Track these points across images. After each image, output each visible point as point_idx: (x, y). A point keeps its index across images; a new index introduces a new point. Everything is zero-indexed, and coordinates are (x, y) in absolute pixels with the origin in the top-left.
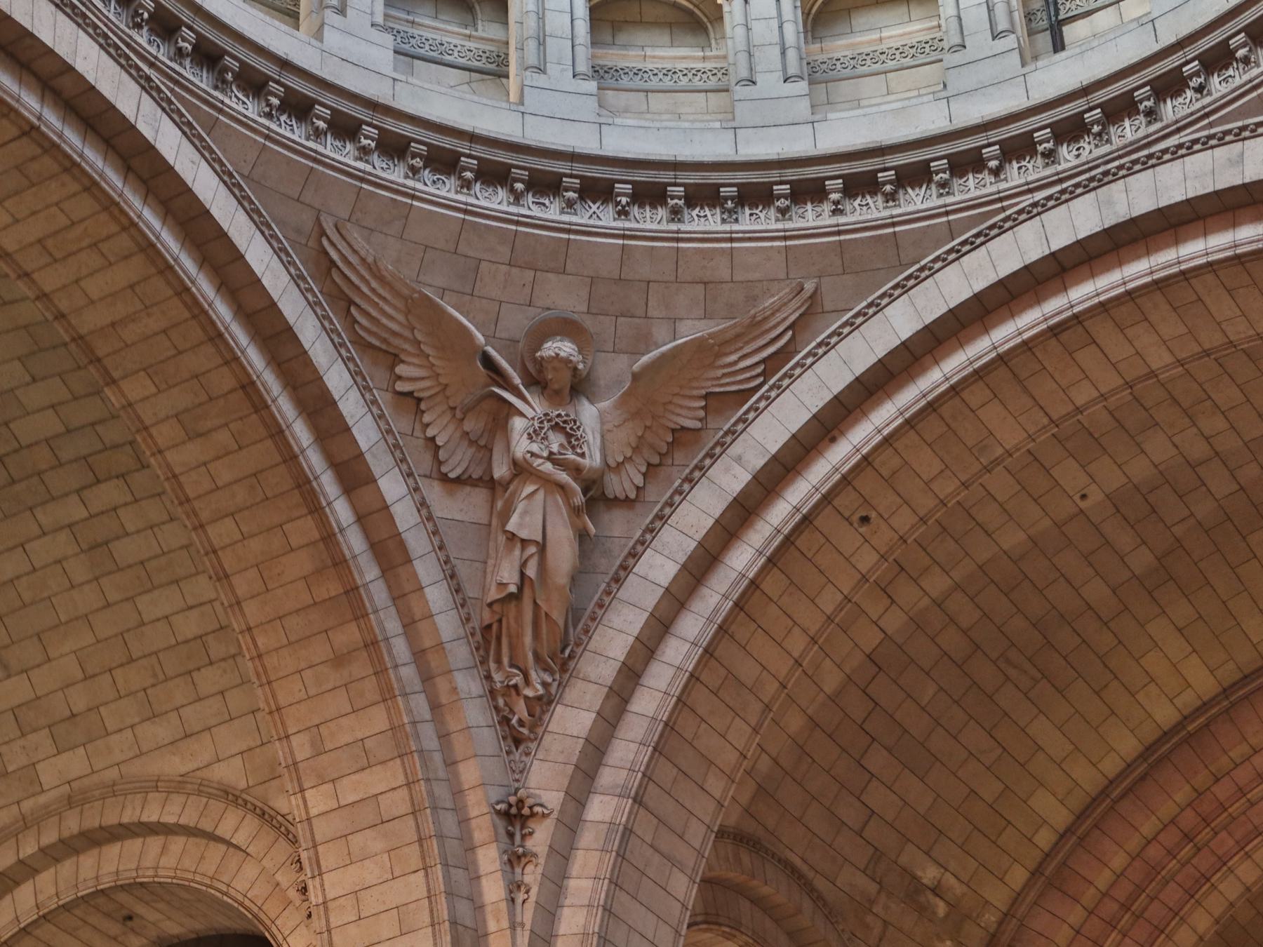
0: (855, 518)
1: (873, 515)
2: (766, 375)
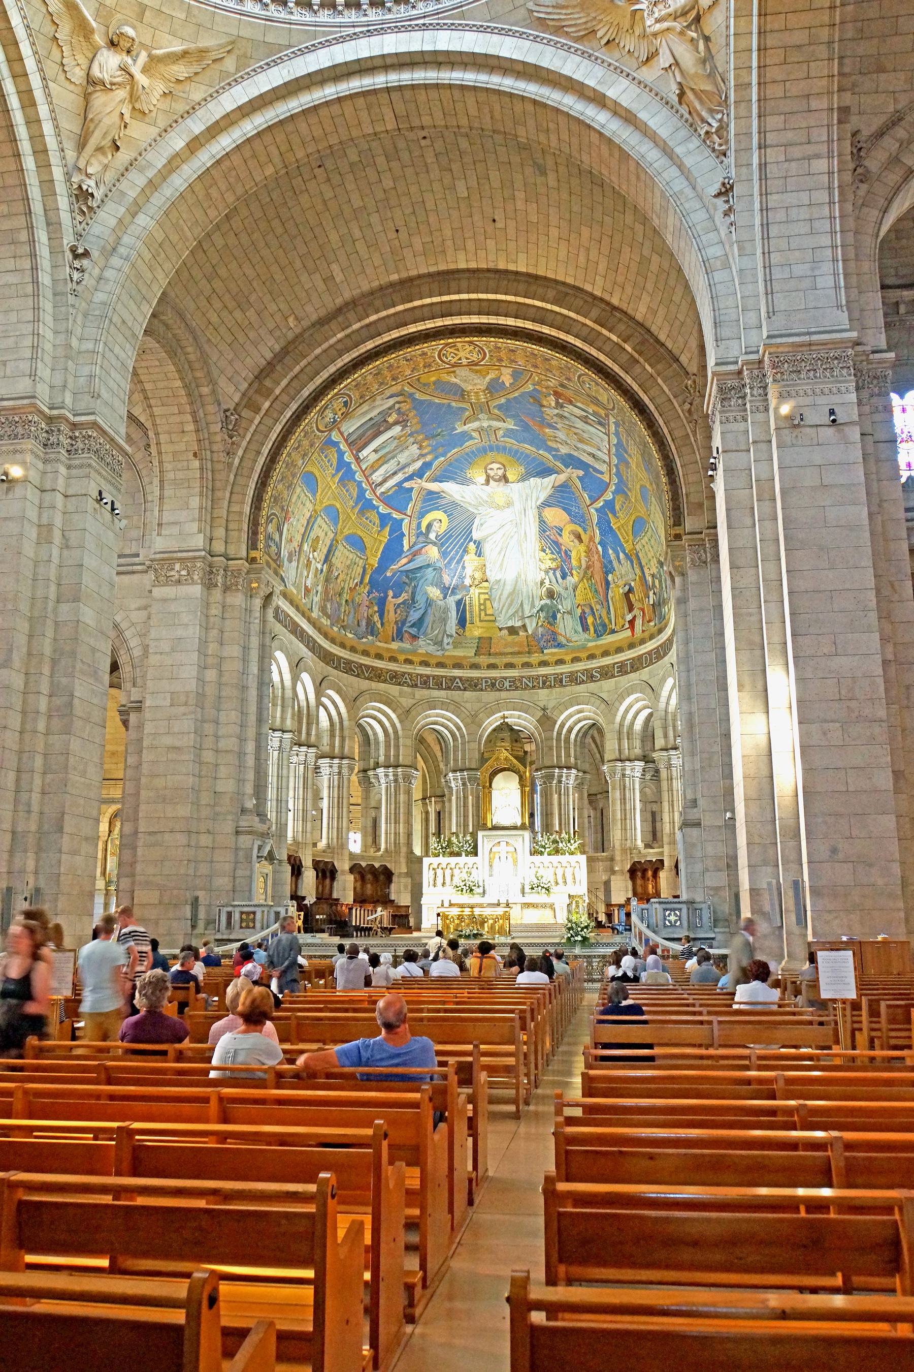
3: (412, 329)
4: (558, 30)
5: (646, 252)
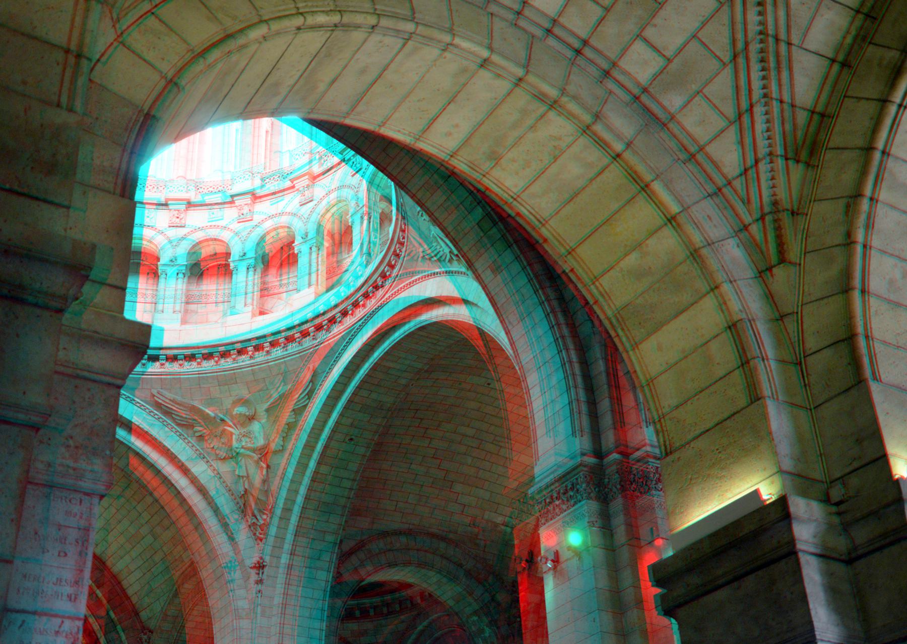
0: (347, 440)
1: (353, 437)
2: (309, 399)
4: (168, 413)
5: (145, 530)
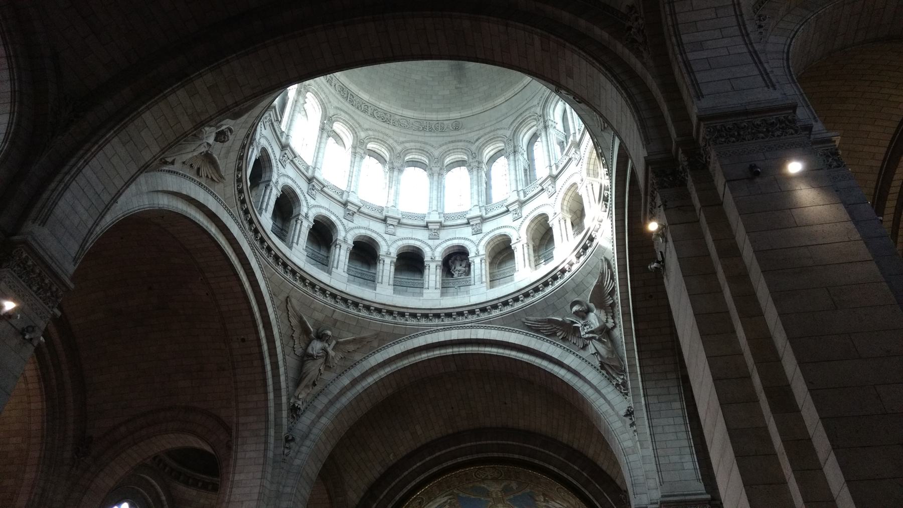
2: (613, 281)
3: (460, 460)
4: (537, 331)
